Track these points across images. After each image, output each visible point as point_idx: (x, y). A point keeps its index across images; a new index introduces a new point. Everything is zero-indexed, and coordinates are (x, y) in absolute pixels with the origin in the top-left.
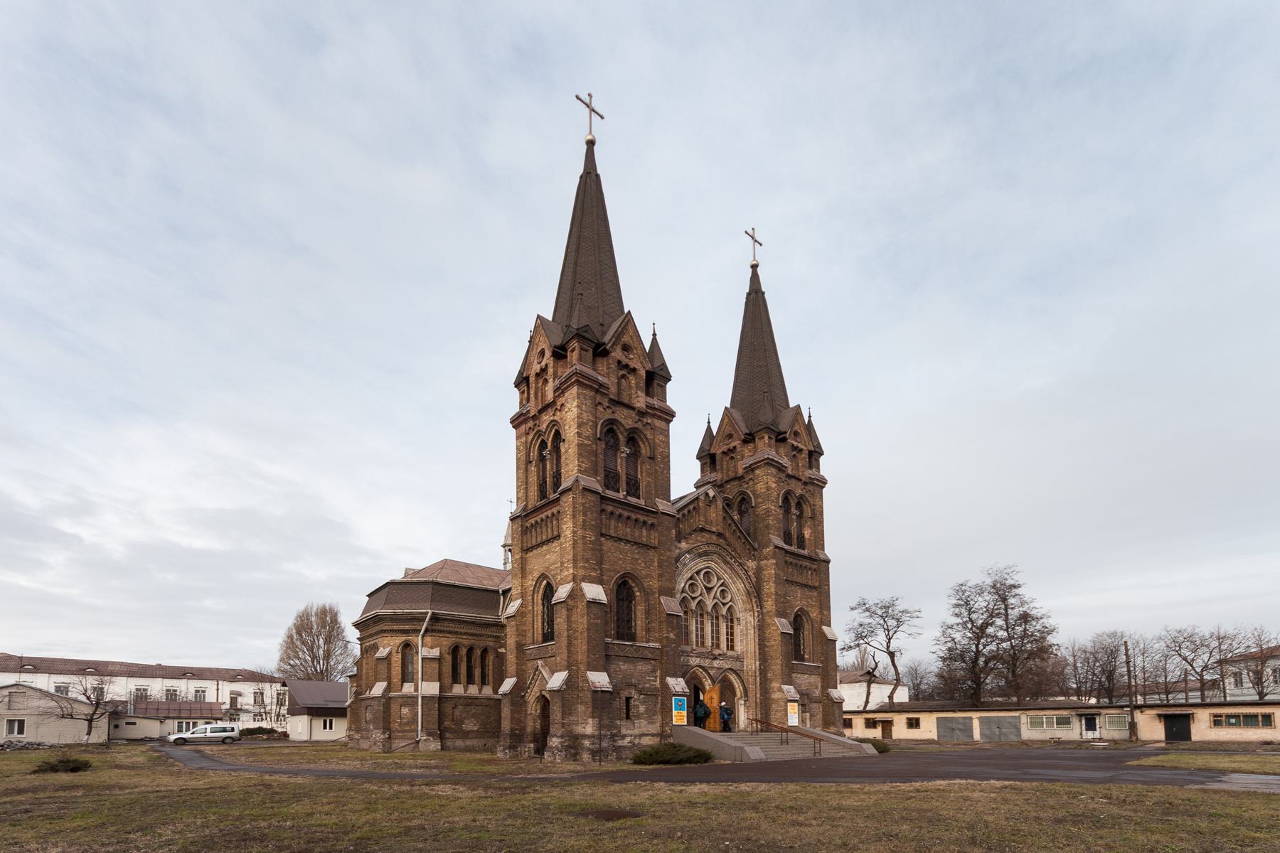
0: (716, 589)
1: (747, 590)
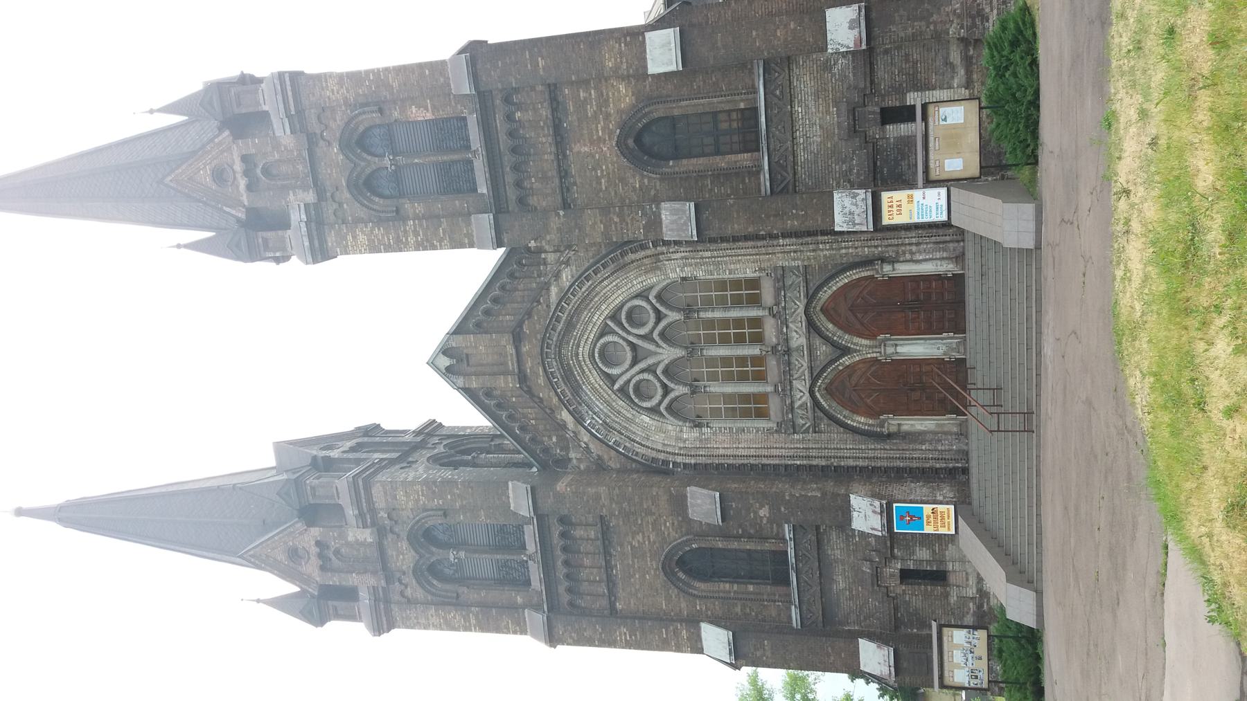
0: (631, 338)
1: (612, 274)
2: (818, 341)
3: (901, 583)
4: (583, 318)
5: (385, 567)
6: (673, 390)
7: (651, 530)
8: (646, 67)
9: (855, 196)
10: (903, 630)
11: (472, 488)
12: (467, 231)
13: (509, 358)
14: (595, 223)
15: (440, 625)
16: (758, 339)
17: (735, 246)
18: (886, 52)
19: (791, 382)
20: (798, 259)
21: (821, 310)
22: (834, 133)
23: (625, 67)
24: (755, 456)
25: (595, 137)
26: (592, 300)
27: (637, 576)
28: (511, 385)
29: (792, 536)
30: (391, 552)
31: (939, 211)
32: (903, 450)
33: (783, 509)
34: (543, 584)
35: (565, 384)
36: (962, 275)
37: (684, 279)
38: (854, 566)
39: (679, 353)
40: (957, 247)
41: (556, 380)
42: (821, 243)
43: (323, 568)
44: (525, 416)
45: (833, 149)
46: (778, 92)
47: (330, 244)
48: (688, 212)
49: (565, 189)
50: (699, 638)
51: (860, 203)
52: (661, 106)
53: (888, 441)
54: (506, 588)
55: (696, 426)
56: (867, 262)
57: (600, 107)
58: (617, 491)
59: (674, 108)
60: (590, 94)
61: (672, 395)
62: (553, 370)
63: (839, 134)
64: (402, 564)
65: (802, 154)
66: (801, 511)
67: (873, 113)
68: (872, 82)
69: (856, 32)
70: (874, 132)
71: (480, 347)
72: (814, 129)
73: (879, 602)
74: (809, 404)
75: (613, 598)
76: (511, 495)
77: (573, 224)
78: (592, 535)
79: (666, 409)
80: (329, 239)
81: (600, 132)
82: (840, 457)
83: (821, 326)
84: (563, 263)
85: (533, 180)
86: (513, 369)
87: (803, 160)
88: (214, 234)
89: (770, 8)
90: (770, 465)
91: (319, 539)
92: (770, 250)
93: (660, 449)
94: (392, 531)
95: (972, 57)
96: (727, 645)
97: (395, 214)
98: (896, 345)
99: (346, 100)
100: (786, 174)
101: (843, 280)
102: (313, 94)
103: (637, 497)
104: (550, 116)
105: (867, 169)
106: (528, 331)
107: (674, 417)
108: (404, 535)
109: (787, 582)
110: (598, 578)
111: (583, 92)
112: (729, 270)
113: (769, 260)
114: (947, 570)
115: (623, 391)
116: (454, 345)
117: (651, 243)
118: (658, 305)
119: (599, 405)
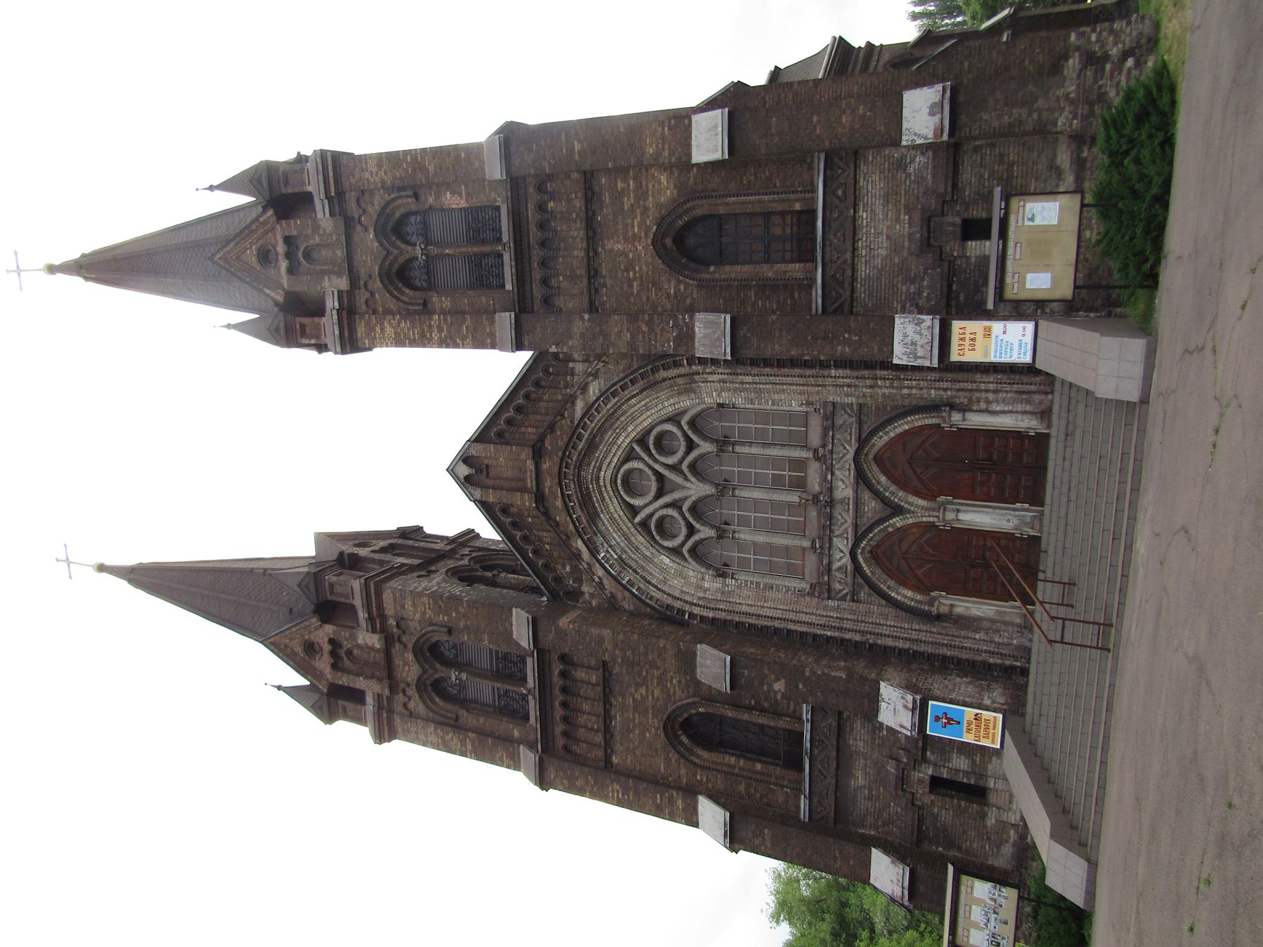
0: (657, 467)
1: (642, 391)
2: (866, 495)
3: (931, 792)
4: (607, 438)
5: (391, 676)
6: (699, 531)
7: (655, 684)
8: (689, 156)
9: (918, 324)
10: (926, 846)
11: (477, 608)
12: (491, 331)
13: (529, 474)
14: (622, 331)
15: (438, 744)
16: (800, 484)
17: (780, 373)
18: (976, 149)
19: (831, 539)
20: (851, 396)
21: (875, 458)
22: (903, 247)
23: (666, 155)
24: (781, 619)
25: (630, 234)
26: (618, 419)
27: (637, 732)
28: (527, 504)
29: (809, 717)
30: (398, 661)
31: (1023, 351)
32: (953, 636)
33: (801, 686)
34: (539, 722)
35: (582, 509)
36: (1047, 436)
37: (721, 405)
38: (878, 762)
39: (706, 489)
40: (1043, 400)
41: (572, 504)
42: (880, 379)
43: (335, 667)
44: (540, 539)
45: (901, 265)
46: (840, 193)
47: (359, 335)
48: (723, 326)
49: (593, 291)
50: (695, 811)
51: (925, 332)
52: (705, 201)
53: (937, 623)
54: (504, 719)
55: (719, 576)
56: (933, 407)
57: (637, 198)
58: (621, 637)
59: (720, 205)
60: (629, 184)
61: (696, 537)
62: (570, 493)
63: (909, 249)
64: (408, 676)
65: (863, 269)
66: (821, 692)
67: (953, 224)
68: (955, 186)
69: (937, 118)
70: (953, 248)
71: (501, 458)
72: (880, 240)
73: (902, 809)
74: (849, 567)
75: (609, 751)
76: (514, 623)
77: (597, 330)
78: (594, 679)
79: (689, 551)
80: (359, 330)
81: (636, 228)
82: (878, 634)
83: (872, 478)
84: (590, 374)
85: (561, 278)
86: (532, 486)
87: (863, 277)
88: (258, 316)
89: (839, 92)
90: (796, 631)
91: (332, 636)
92: (820, 381)
93: (677, 595)
94: (400, 641)
95: (1085, 160)
96: (722, 826)
97: (421, 307)
98: (958, 511)
99: (383, 182)
100: (842, 291)
101: (902, 426)
102: (354, 177)
103: (642, 647)
104: (583, 208)
105: (939, 293)
106: (549, 447)
107: (697, 562)
108: (410, 646)
109: (802, 770)
110: (595, 727)
111: (621, 181)
112: (772, 400)
113: (818, 393)
114: (987, 786)
115: (644, 524)
116: (474, 454)
117: (685, 361)
118: (690, 433)
119: (617, 538)
